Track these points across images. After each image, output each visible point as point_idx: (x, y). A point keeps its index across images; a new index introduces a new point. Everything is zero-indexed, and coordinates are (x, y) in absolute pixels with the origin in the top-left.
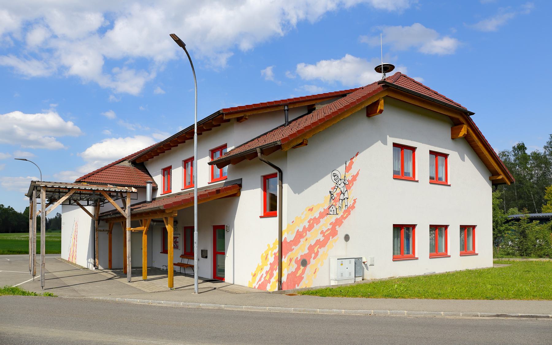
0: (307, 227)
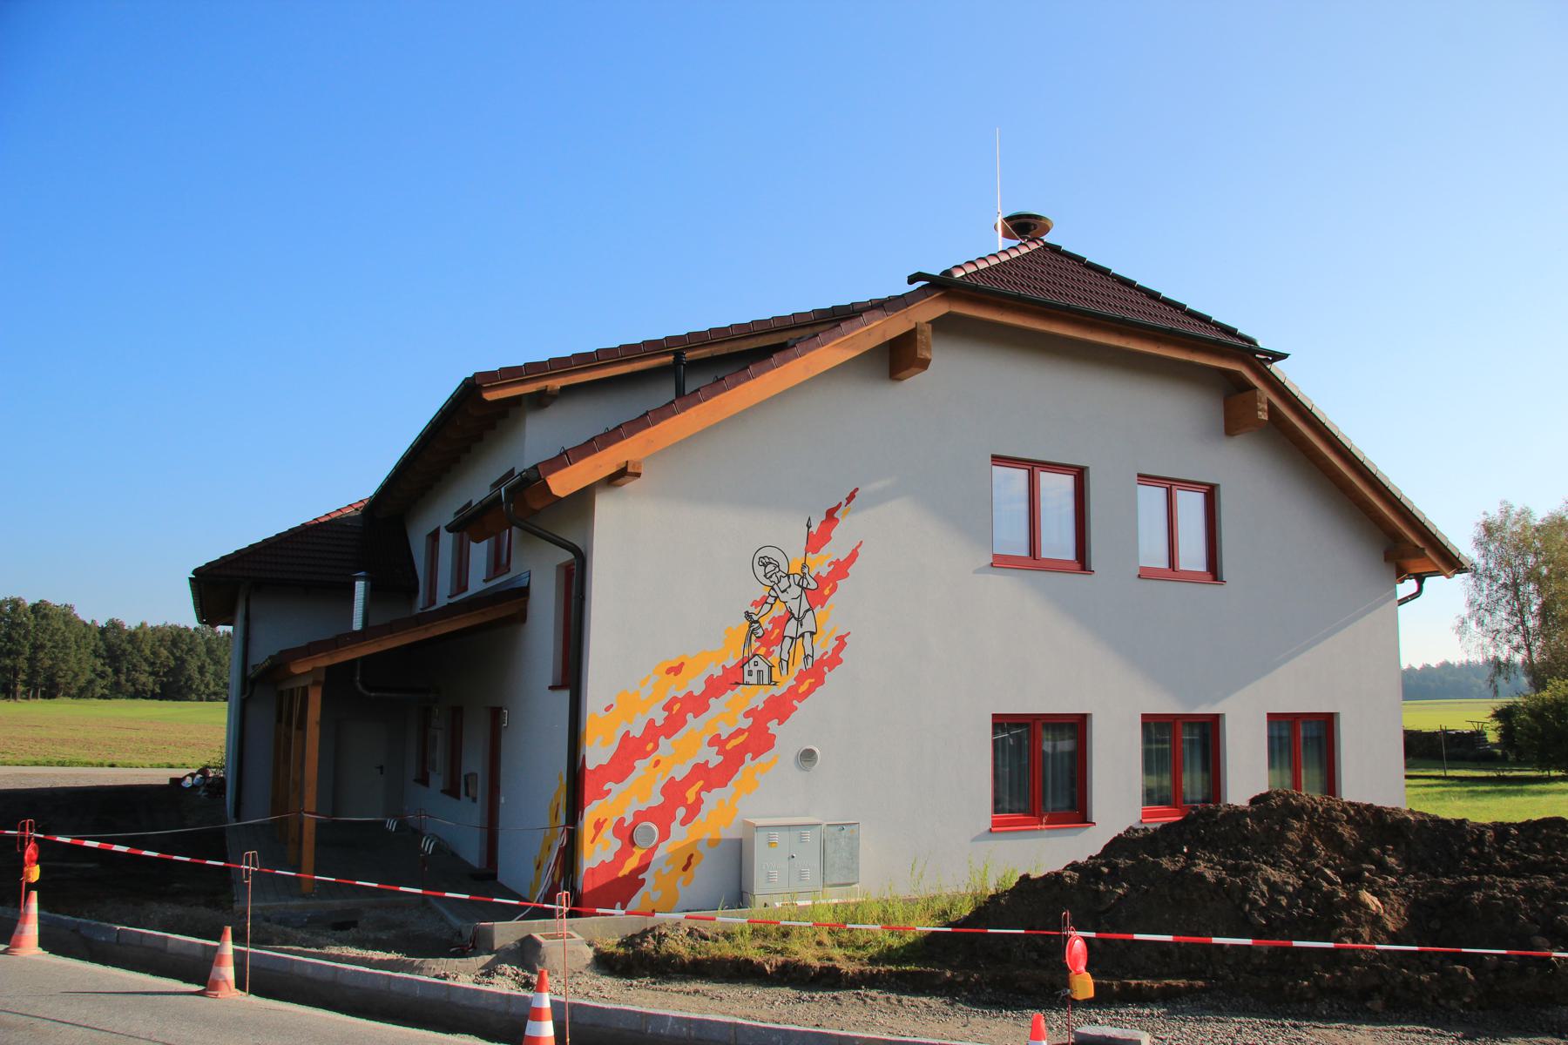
0: (659, 722)
